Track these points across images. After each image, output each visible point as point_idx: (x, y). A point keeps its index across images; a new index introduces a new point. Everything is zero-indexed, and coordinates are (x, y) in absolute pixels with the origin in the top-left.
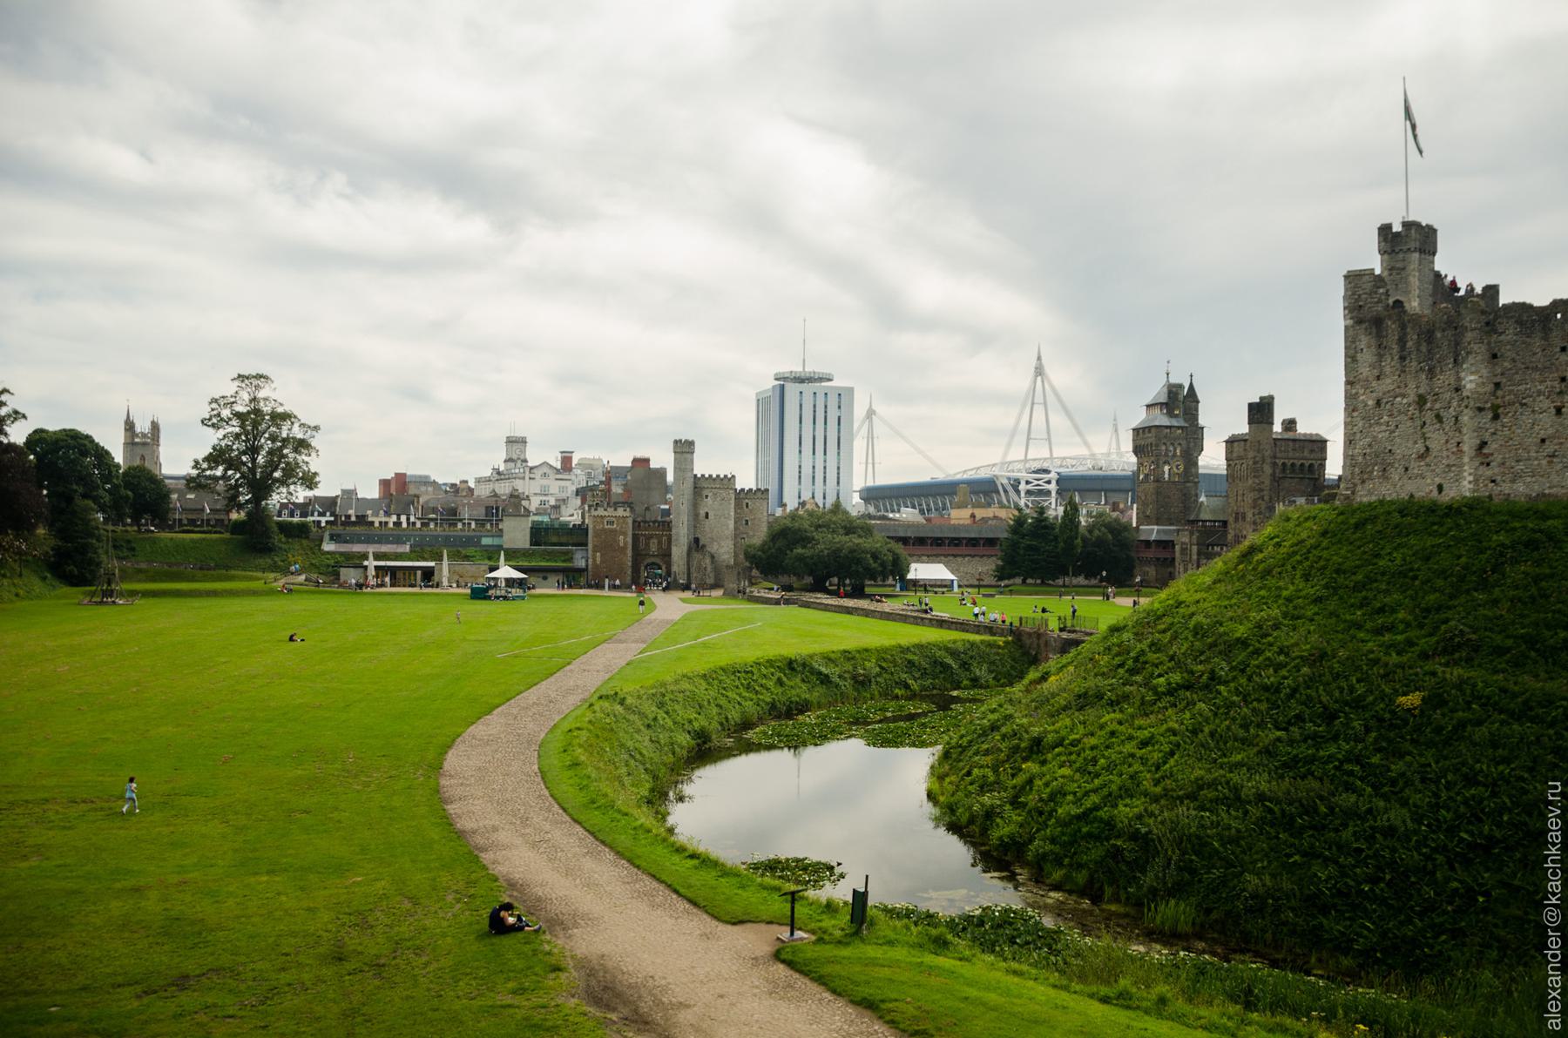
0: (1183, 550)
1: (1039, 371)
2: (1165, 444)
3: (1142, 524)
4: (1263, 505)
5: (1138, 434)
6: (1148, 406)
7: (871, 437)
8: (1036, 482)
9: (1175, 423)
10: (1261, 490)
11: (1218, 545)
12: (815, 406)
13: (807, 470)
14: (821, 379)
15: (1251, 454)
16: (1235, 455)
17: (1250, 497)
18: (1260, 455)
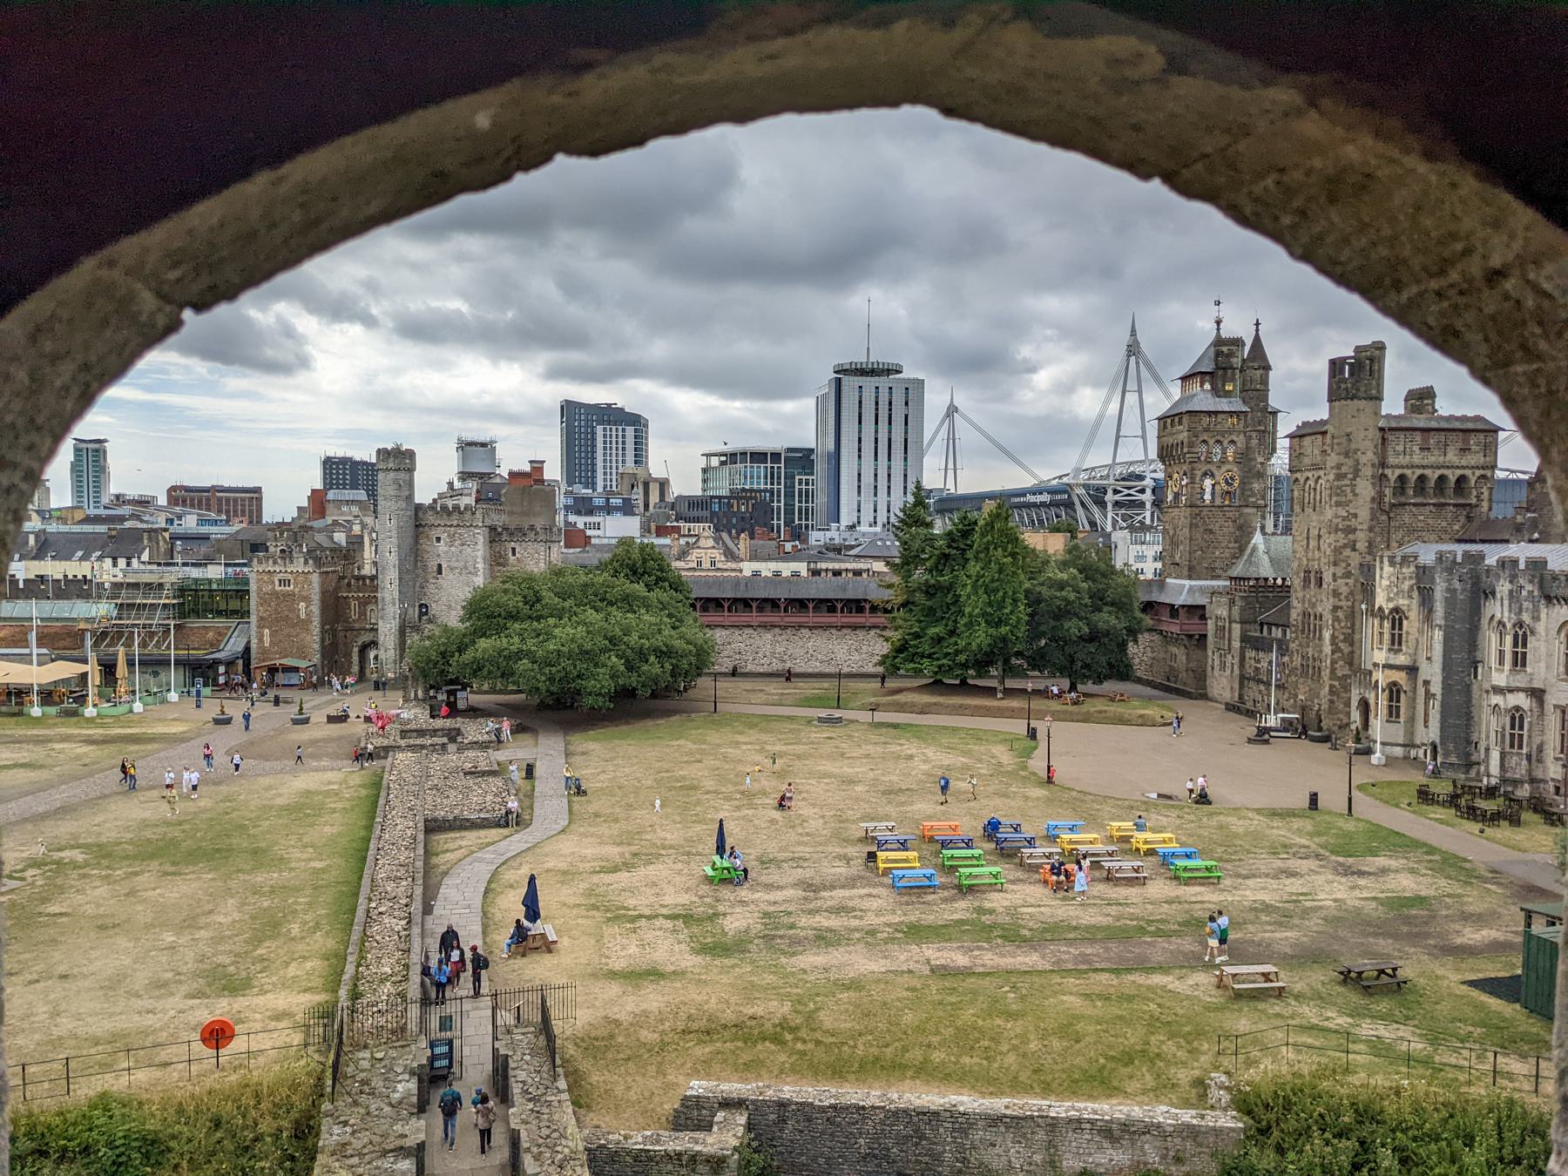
0: (1220, 630)
1: (1133, 349)
2: (1204, 441)
3: (1170, 576)
4: (1355, 560)
5: (1165, 427)
6: (1184, 379)
7: (952, 439)
8: (1126, 491)
9: (1224, 405)
10: (1350, 530)
11: (1277, 626)
12: (877, 403)
13: (867, 478)
14: (888, 371)
15: (1333, 459)
16: (1307, 461)
17: (1329, 541)
18: (1350, 462)
